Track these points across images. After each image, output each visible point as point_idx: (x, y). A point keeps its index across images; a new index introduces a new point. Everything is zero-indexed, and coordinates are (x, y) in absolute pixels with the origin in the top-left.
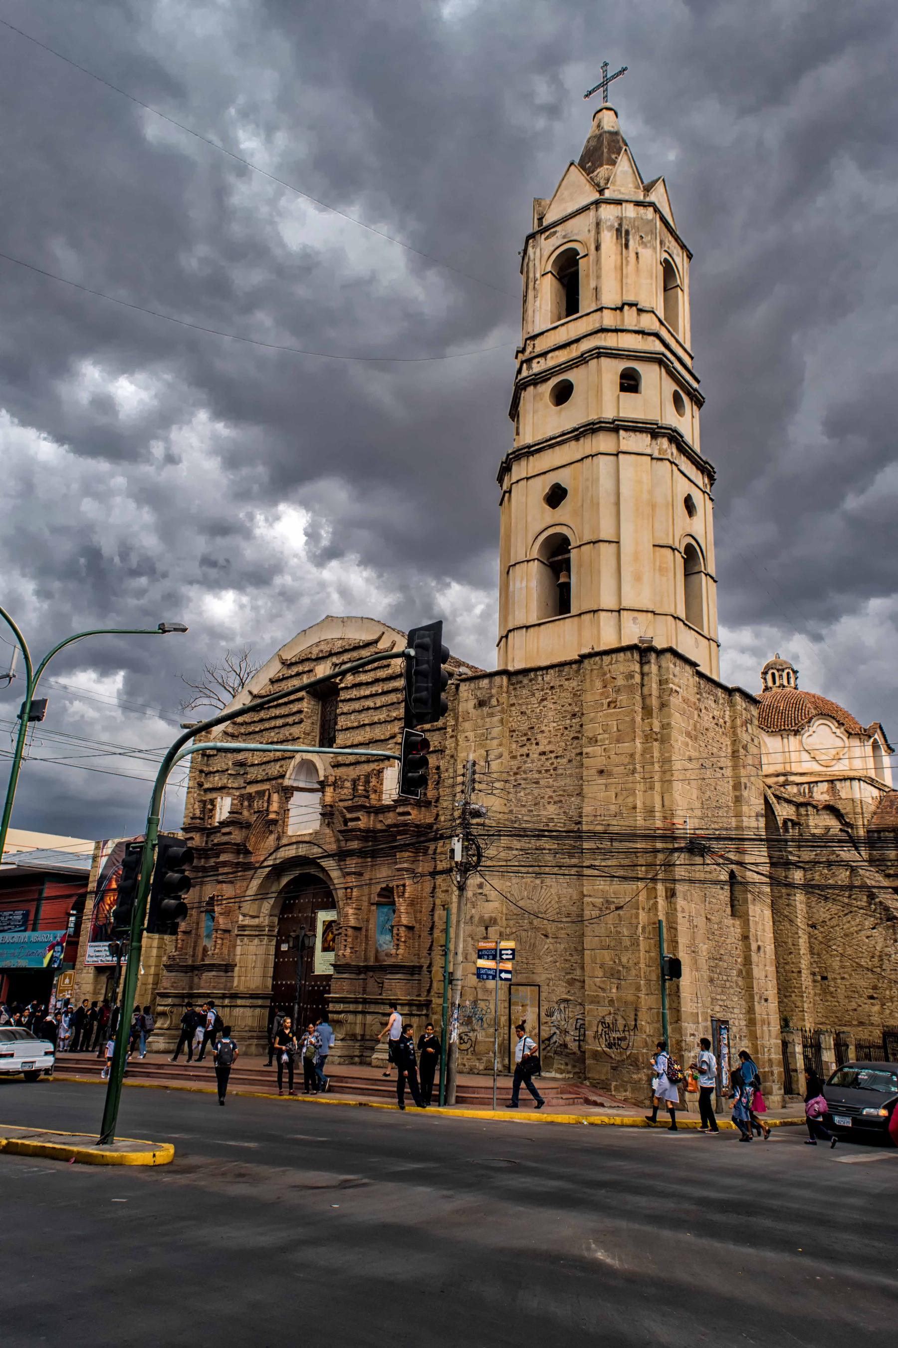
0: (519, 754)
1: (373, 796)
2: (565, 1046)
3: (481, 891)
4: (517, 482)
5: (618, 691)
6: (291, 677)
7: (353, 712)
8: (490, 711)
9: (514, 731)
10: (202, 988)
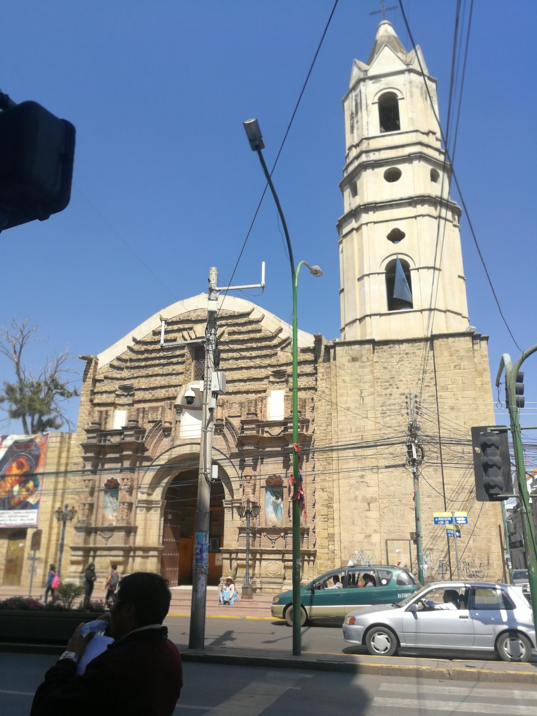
0: (383, 393)
3: (362, 480)
4: (367, 224)
5: (461, 359)
6: (173, 331)
8: (362, 364)
9: (379, 379)
10: (114, 543)
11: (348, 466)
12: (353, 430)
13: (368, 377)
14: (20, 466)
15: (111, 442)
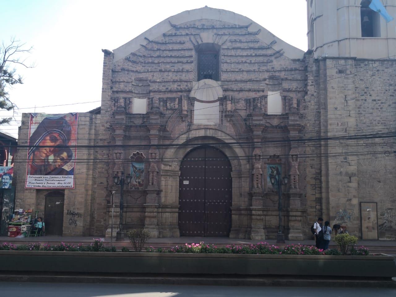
0: (360, 99)
1: (263, 110)
2: (391, 227)
3: (346, 161)
6: (182, 35)
7: (233, 63)
10: (148, 203)
11: (335, 152)
12: (340, 124)
13: (351, 86)
14: (53, 140)
15: (135, 124)
